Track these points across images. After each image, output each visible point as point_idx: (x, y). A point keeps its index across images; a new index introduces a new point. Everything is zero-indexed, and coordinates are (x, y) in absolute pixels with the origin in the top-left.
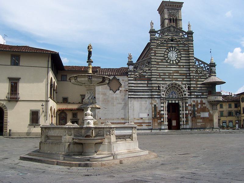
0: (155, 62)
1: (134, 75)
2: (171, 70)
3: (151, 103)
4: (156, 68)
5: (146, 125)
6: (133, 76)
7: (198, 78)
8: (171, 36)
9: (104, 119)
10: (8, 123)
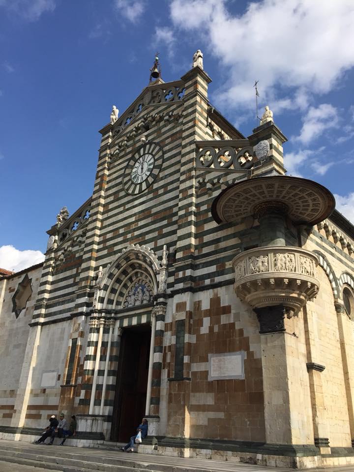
2: (130, 216)
8: (143, 116)
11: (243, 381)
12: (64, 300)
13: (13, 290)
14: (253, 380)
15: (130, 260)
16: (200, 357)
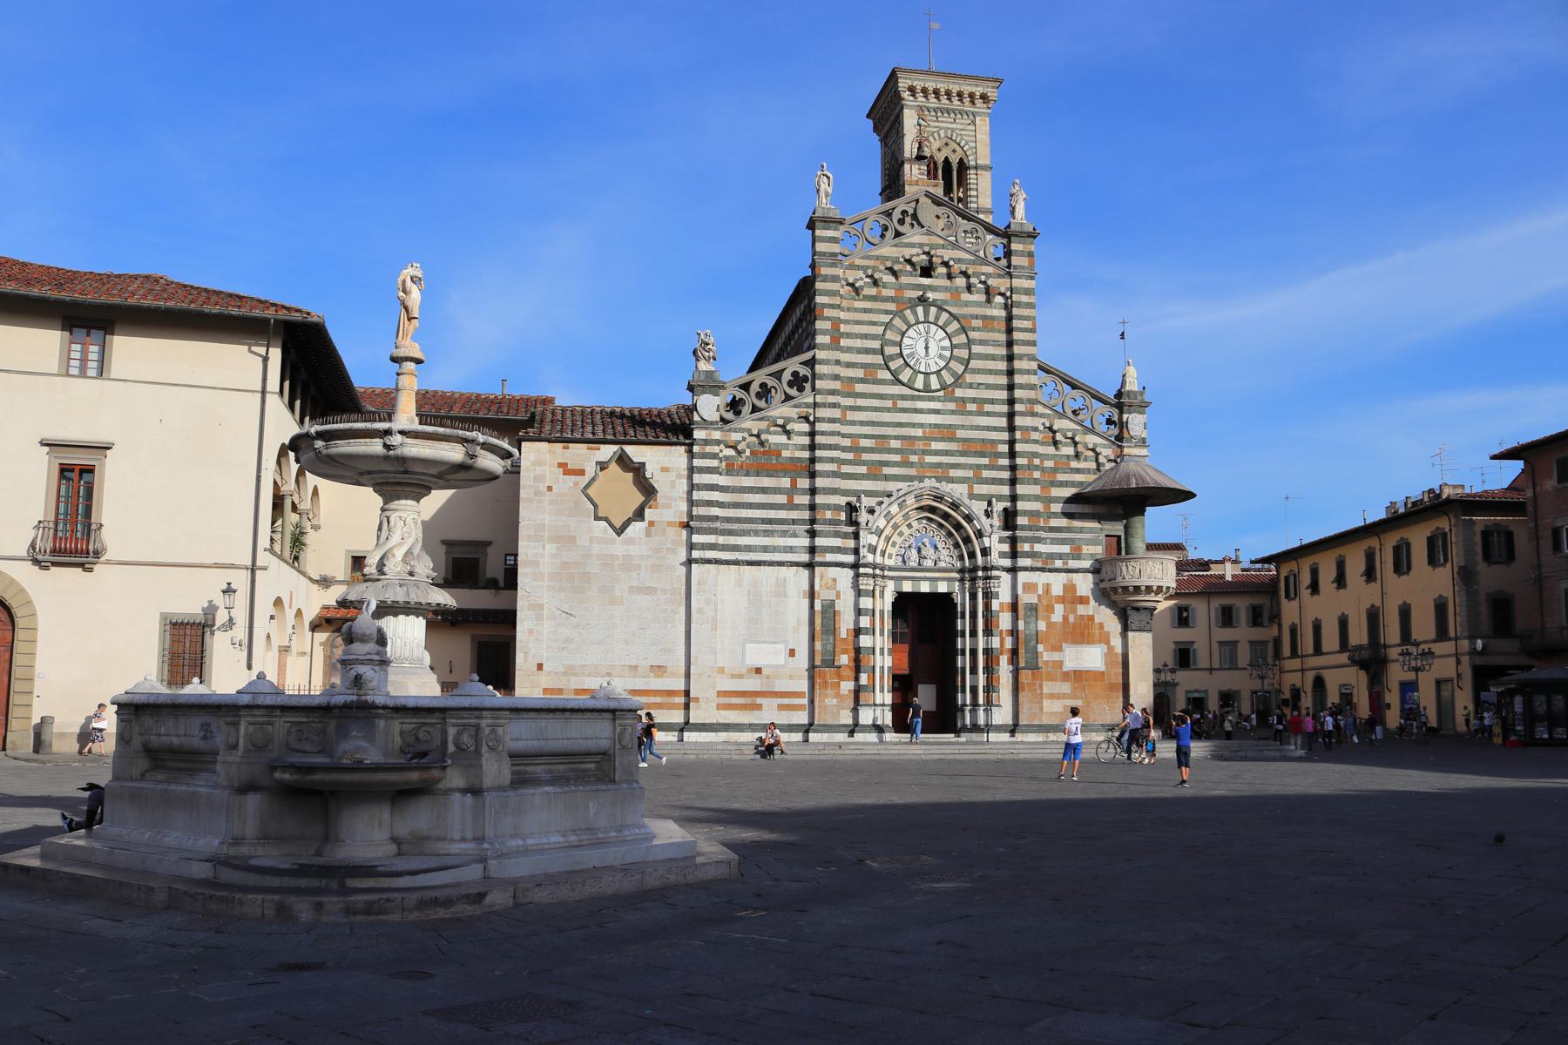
0: (836, 377)
1: (722, 446)
2: (913, 425)
3: (804, 591)
4: (836, 413)
5: (781, 707)
6: (716, 449)
7: (1055, 470)
8: (921, 245)
9: (561, 669)
10: (37, 682)
11: (1103, 672)
13: (581, 472)
14: (1113, 671)
16: (1052, 646)
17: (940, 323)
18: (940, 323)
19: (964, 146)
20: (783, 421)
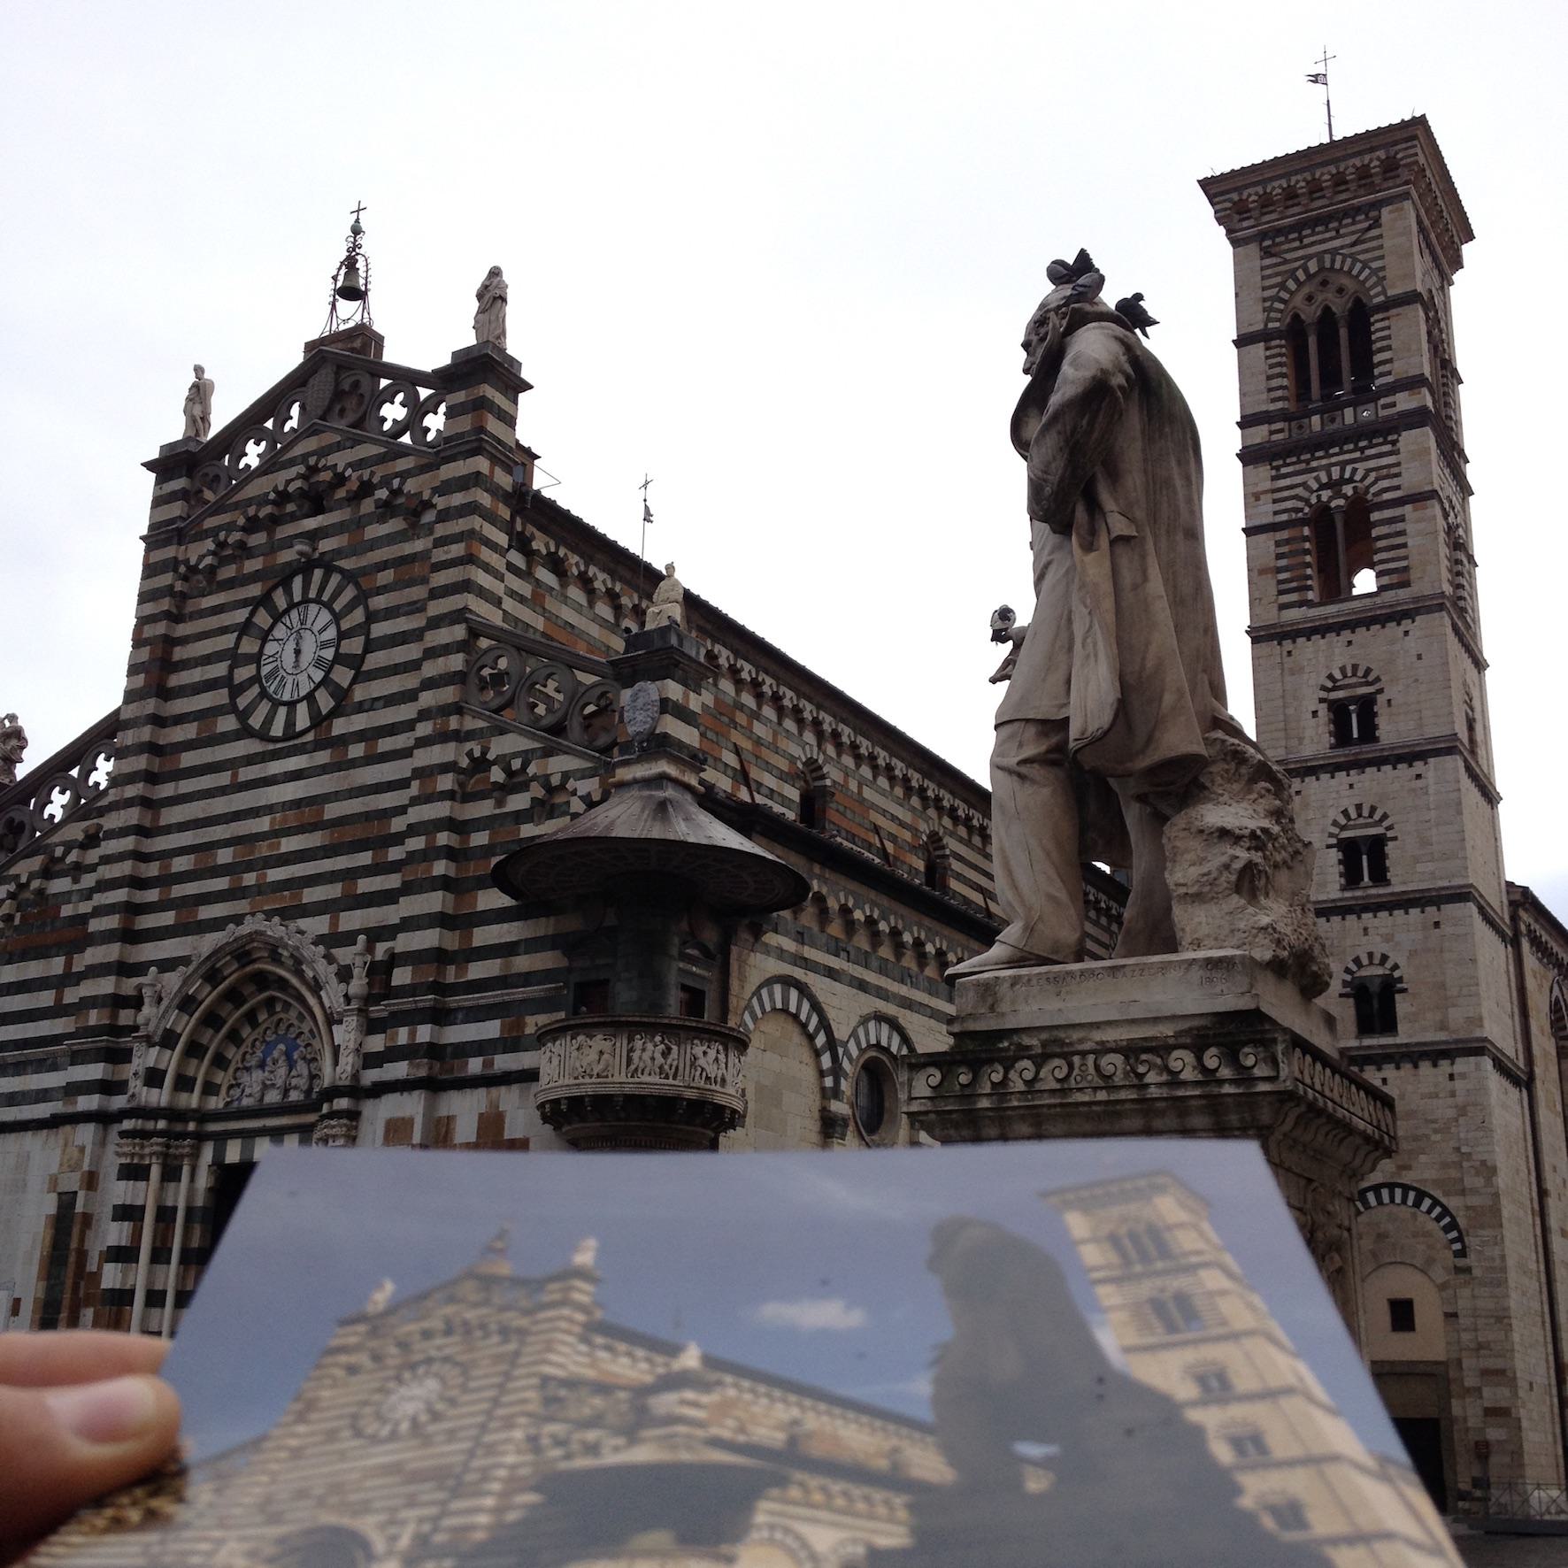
8: (305, 457)
12: (23, 1059)
15: (254, 961)
17: (325, 598)
18: (325, 598)
19: (1360, 272)
20: (62, 848)
